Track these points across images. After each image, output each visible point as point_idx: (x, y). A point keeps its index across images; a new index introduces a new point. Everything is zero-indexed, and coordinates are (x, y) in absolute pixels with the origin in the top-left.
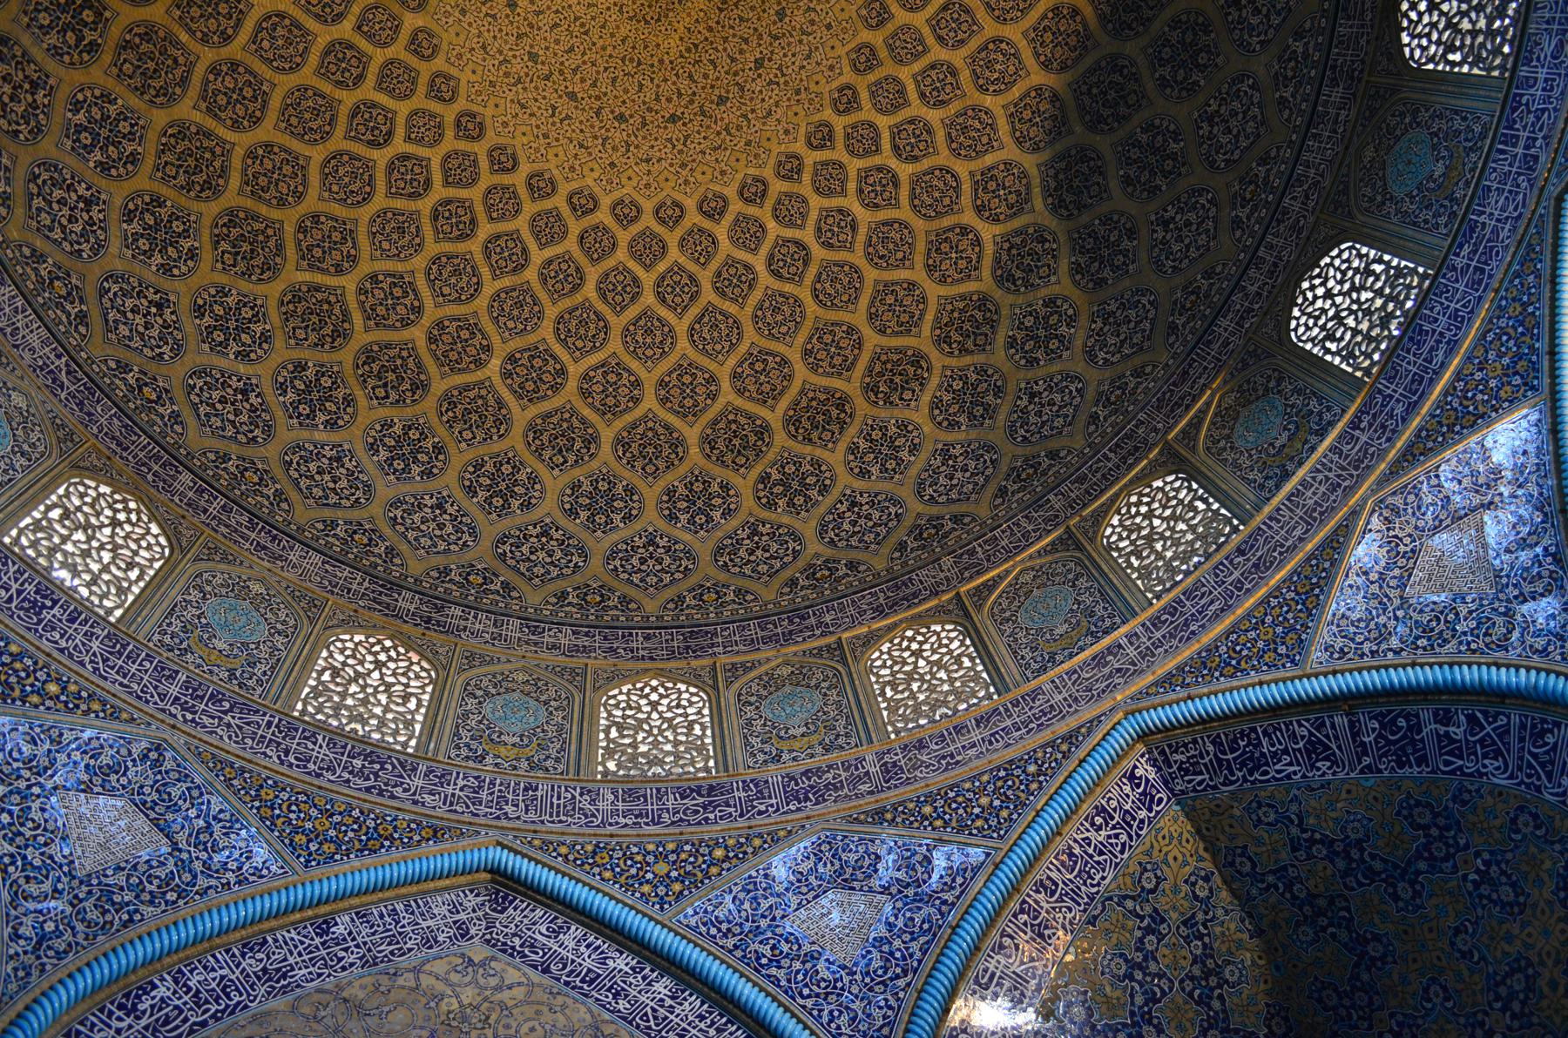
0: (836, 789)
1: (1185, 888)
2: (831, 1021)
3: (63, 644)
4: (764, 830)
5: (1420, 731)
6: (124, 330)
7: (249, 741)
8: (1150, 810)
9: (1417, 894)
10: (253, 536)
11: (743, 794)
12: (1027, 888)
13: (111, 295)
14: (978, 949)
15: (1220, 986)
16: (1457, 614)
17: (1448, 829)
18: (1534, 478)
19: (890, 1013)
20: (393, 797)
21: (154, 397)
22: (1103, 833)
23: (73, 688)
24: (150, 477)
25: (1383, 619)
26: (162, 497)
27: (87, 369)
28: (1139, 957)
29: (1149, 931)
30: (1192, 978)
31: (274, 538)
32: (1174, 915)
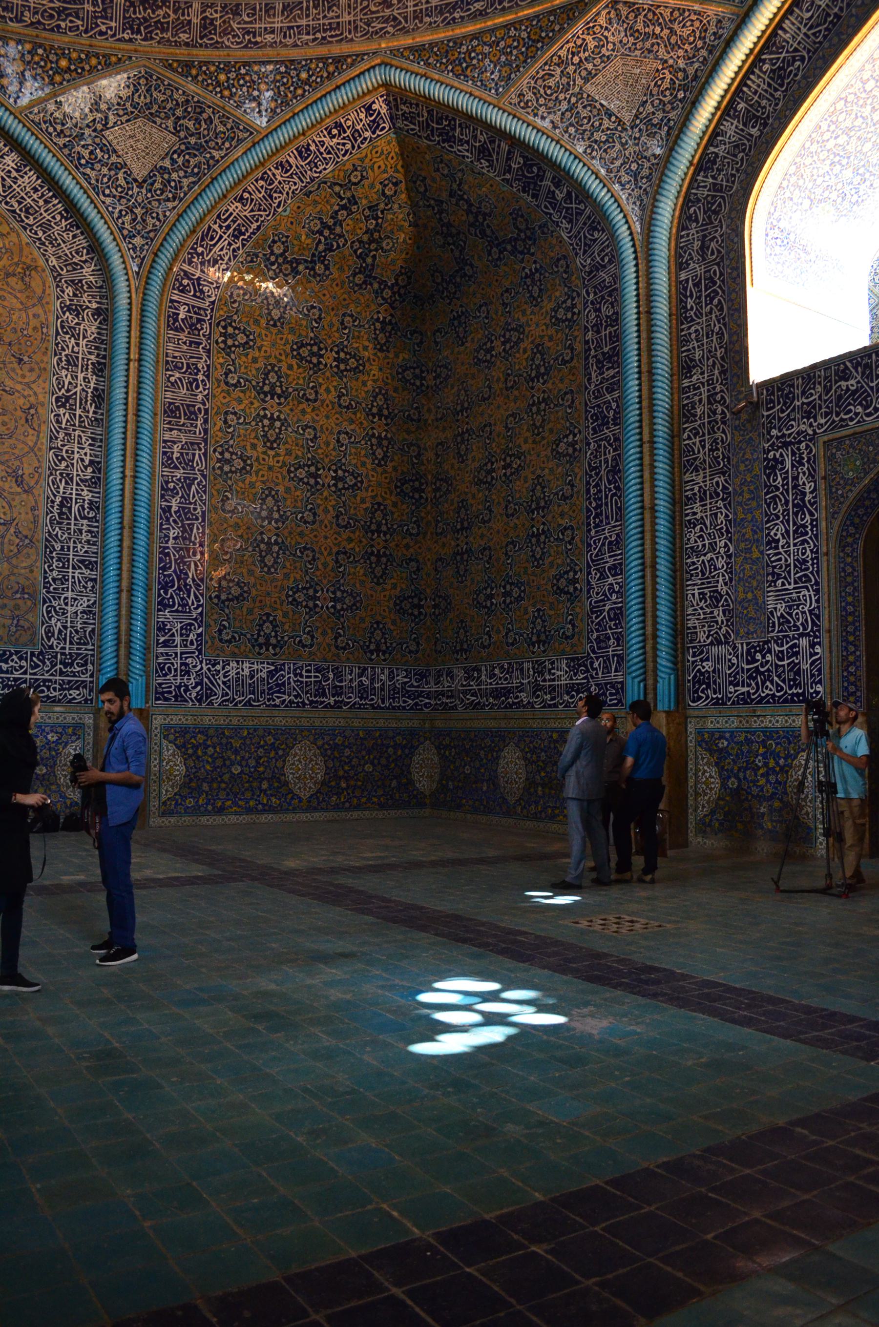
0: (163, 30)
1: (378, 187)
2: (119, 217)
4: (101, 51)
5: (541, 181)
8: (374, 133)
9: (499, 259)
11: (91, 9)
12: (270, 165)
14: (225, 196)
15: (376, 250)
16: (601, 124)
17: (530, 239)
18: (696, 65)
19: (157, 223)
22: (335, 140)
25: (562, 96)
28: (331, 222)
29: (344, 207)
30: (360, 241)
32: (364, 202)
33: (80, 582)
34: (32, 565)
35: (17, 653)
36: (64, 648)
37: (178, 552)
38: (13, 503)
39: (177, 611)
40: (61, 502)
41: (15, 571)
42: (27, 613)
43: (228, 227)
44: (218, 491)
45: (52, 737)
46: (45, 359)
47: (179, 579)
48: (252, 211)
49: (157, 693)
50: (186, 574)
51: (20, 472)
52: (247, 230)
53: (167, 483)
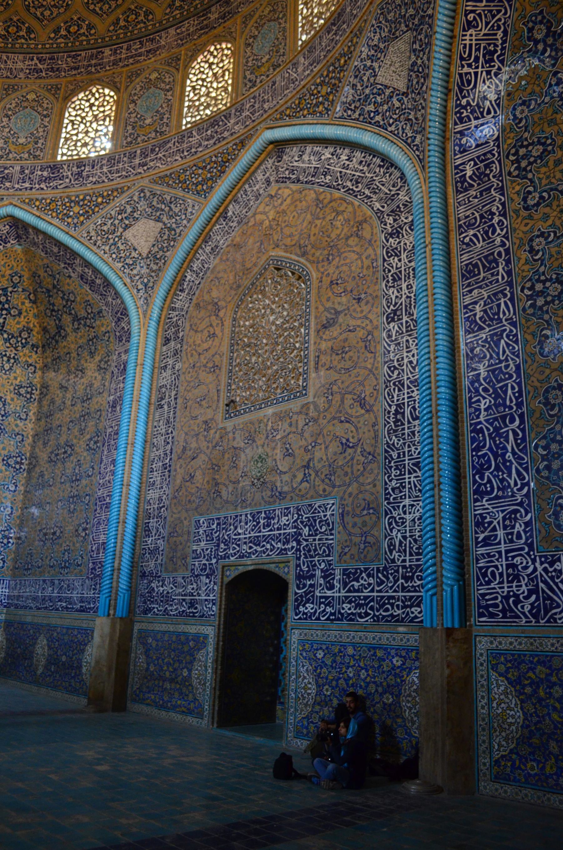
3: (94, 180)
6: (47, 13)
7: (169, 159)
10: (143, 50)
13: (32, 5)
20: (224, 138)
21: (76, 28)
23: (105, 194)
24: (93, 70)
26: (102, 73)
27: (45, 51)
31: (152, 40)
33: (415, 486)
34: (375, 480)
35: (366, 569)
36: (404, 561)
37: (491, 424)
38: (359, 425)
39: (497, 497)
40: (396, 410)
41: (363, 488)
42: (372, 528)
43: (477, 59)
44: (533, 335)
45: (397, 662)
46: (377, 287)
47: (496, 456)
48: (487, 24)
49: (480, 607)
50: (505, 448)
51: (363, 396)
52: (496, 45)
53: (472, 350)
